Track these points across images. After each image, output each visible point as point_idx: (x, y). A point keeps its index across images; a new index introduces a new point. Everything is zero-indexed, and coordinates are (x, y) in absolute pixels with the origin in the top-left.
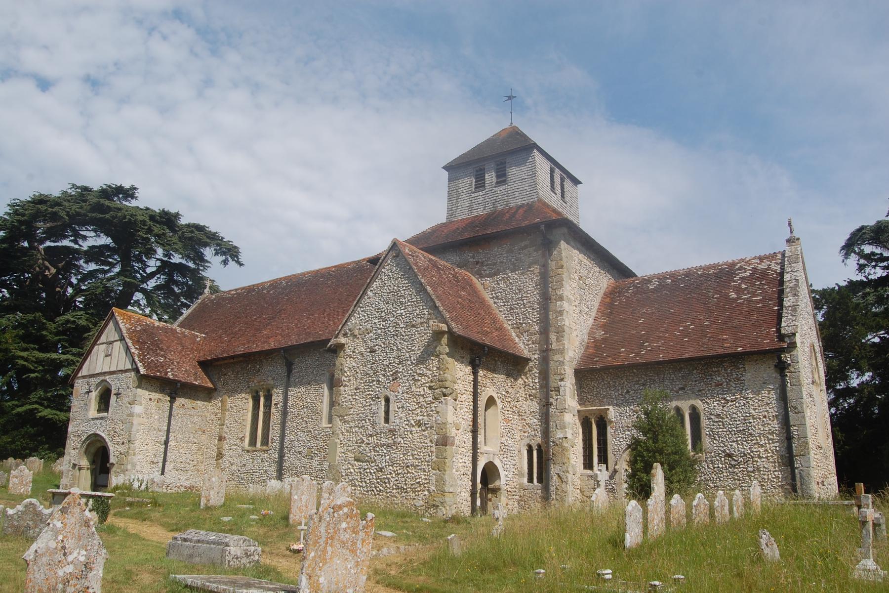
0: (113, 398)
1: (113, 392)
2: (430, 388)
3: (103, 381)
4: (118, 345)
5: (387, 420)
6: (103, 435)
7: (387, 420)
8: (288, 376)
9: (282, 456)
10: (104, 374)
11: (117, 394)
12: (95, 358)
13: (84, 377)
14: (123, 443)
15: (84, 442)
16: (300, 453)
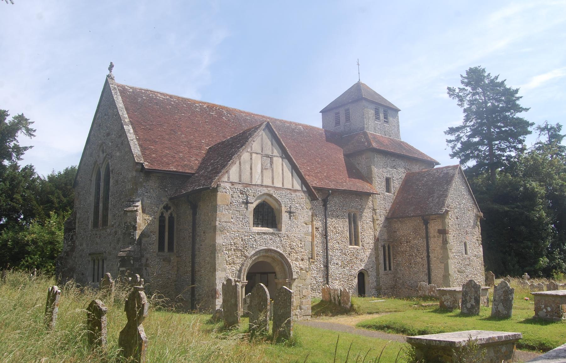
0: (285, 216)
1: (284, 209)
2: (477, 240)
3: (264, 194)
4: (278, 162)
5: (466, 253)
6: (278, 250)
7: (466, 253)
8: (326, 209)
9: (326, 267)
10: (267, 187)
11: (290, 213)
12: (248, 167)
13: (233, 184)
14: (302, 260)
15: (251, 258)
16: (337, 264)
